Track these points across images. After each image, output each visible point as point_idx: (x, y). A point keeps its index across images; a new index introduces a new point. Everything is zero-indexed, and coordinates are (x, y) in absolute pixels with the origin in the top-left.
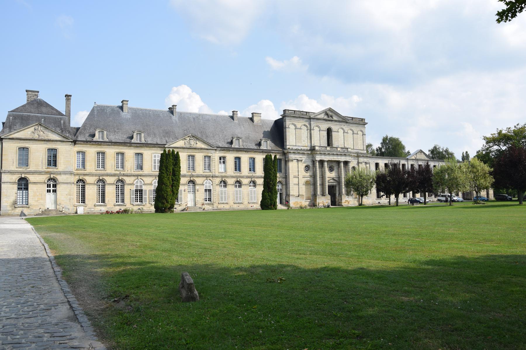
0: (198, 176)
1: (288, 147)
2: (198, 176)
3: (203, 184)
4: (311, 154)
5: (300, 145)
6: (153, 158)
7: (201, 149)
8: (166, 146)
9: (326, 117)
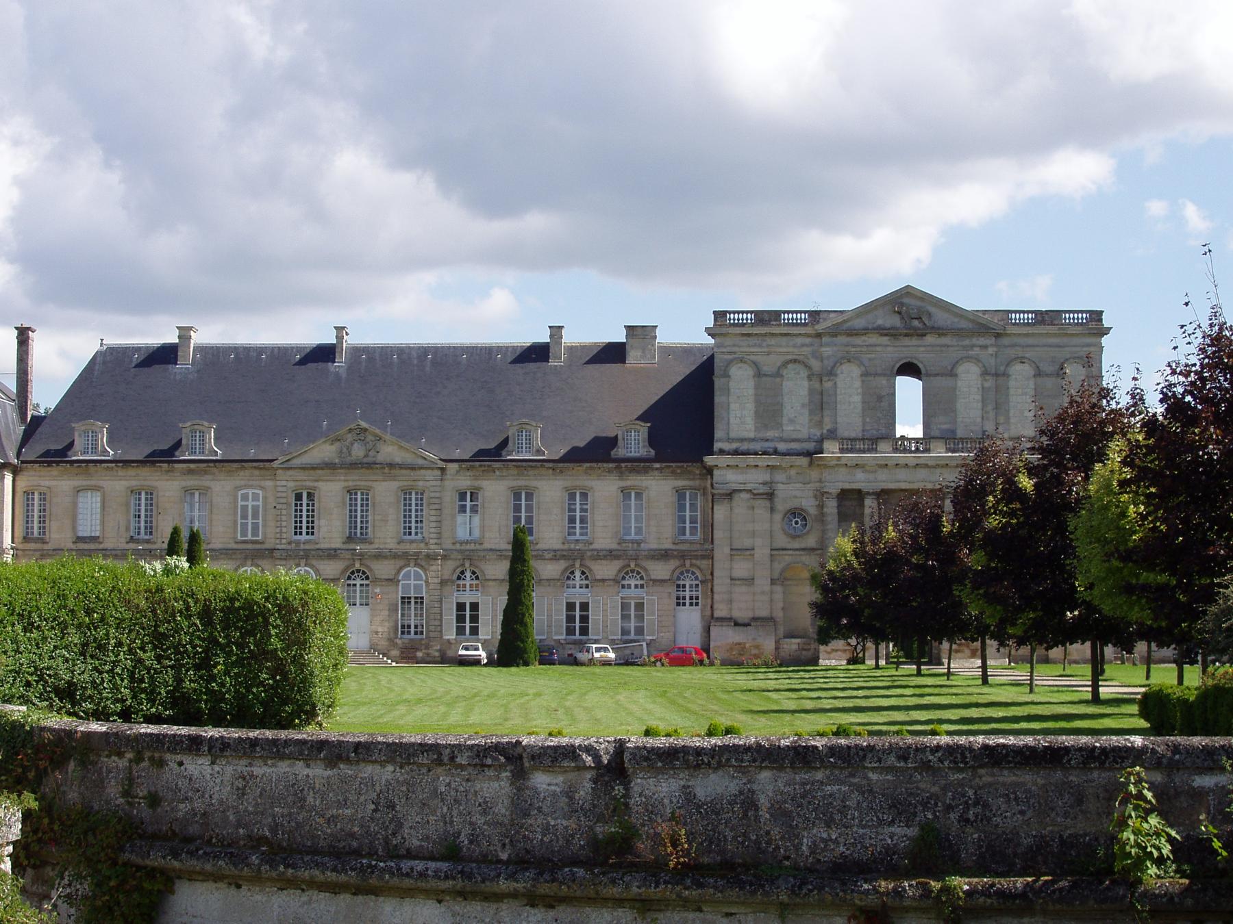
0: (379, 556)
1: (717, 446)
2: (379, 556)
3: (393, 581)
4: (811, 464)
5: (770, 434)
6: (240, 503)
7: (391, 466)
8: (275, 464)
9: (895, 321)
